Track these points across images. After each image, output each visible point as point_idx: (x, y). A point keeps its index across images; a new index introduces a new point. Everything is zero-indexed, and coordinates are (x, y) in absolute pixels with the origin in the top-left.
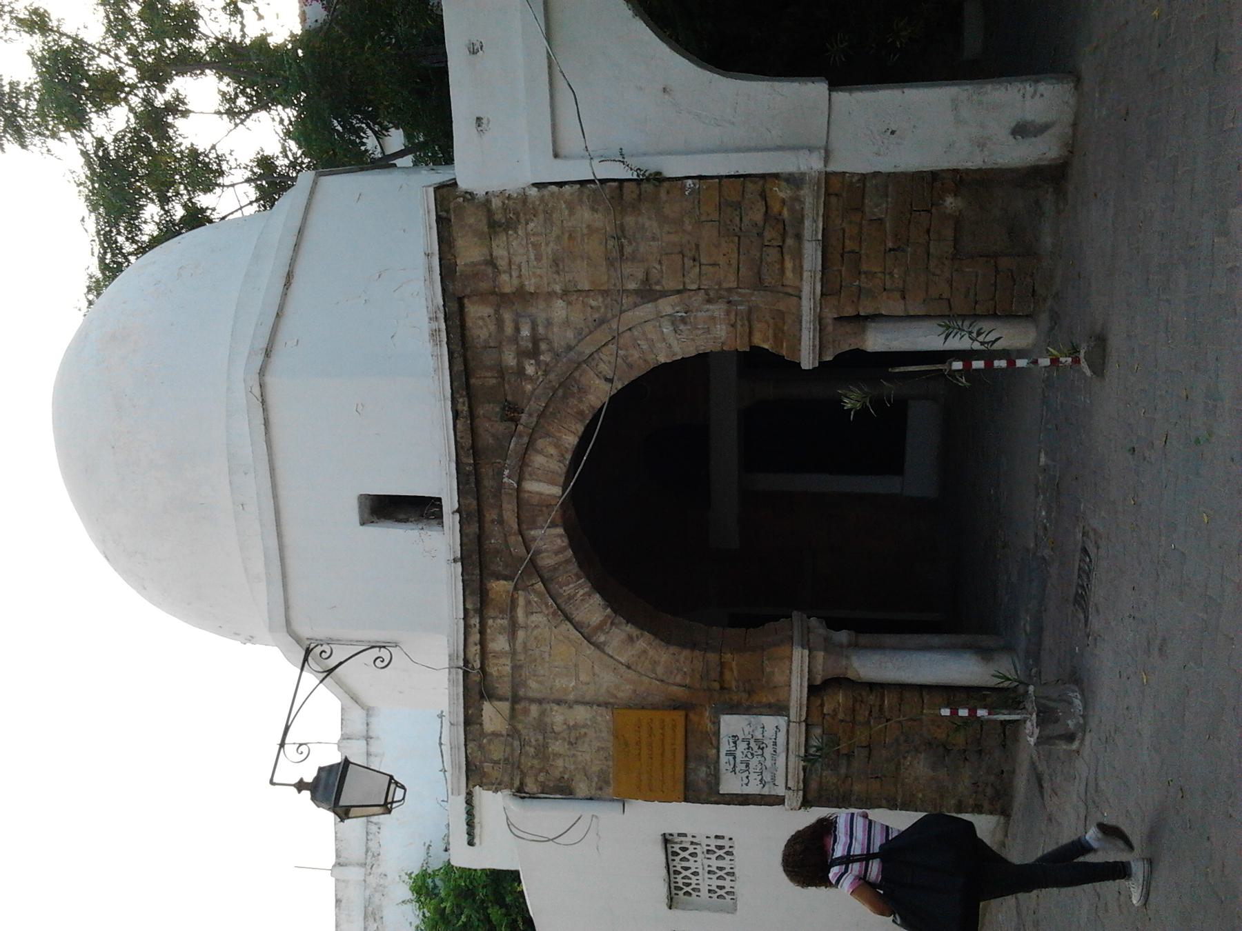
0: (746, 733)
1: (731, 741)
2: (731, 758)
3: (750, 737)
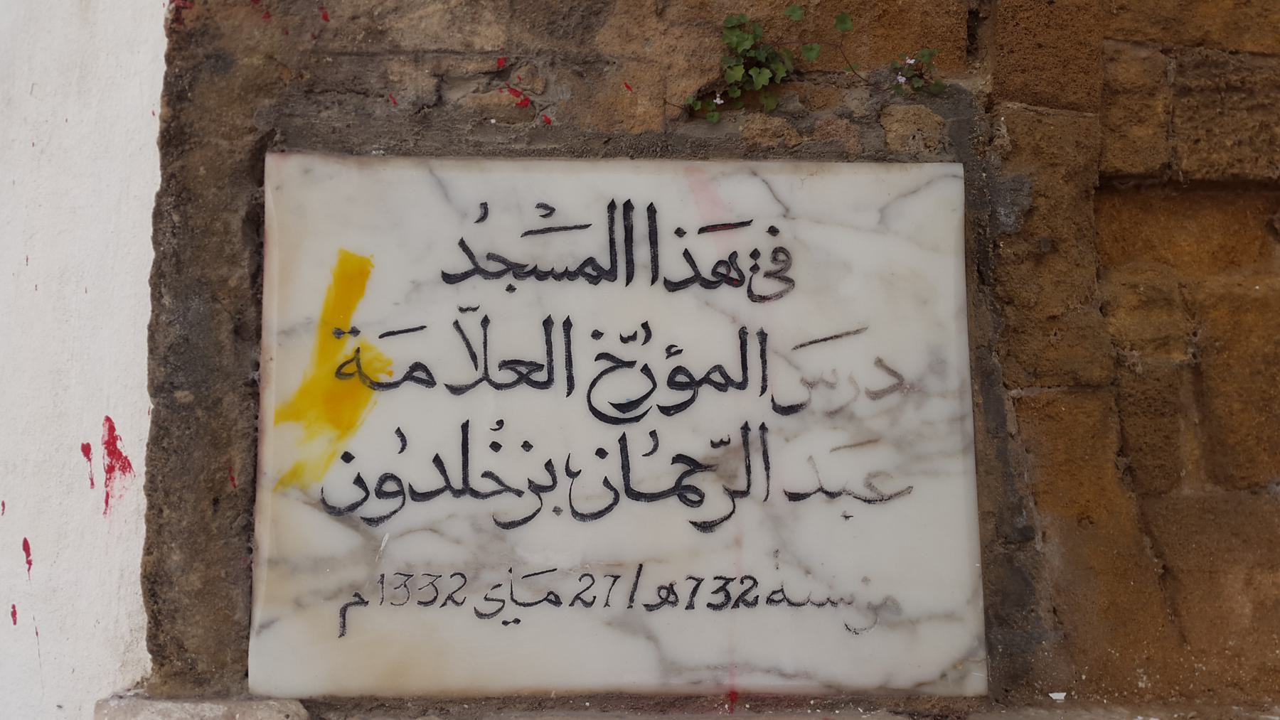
0: (818, 361)
1: (742, 242)
2: (593, 244)
3: (788, 391)
